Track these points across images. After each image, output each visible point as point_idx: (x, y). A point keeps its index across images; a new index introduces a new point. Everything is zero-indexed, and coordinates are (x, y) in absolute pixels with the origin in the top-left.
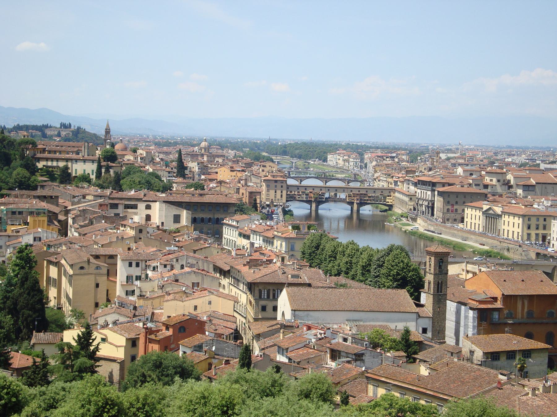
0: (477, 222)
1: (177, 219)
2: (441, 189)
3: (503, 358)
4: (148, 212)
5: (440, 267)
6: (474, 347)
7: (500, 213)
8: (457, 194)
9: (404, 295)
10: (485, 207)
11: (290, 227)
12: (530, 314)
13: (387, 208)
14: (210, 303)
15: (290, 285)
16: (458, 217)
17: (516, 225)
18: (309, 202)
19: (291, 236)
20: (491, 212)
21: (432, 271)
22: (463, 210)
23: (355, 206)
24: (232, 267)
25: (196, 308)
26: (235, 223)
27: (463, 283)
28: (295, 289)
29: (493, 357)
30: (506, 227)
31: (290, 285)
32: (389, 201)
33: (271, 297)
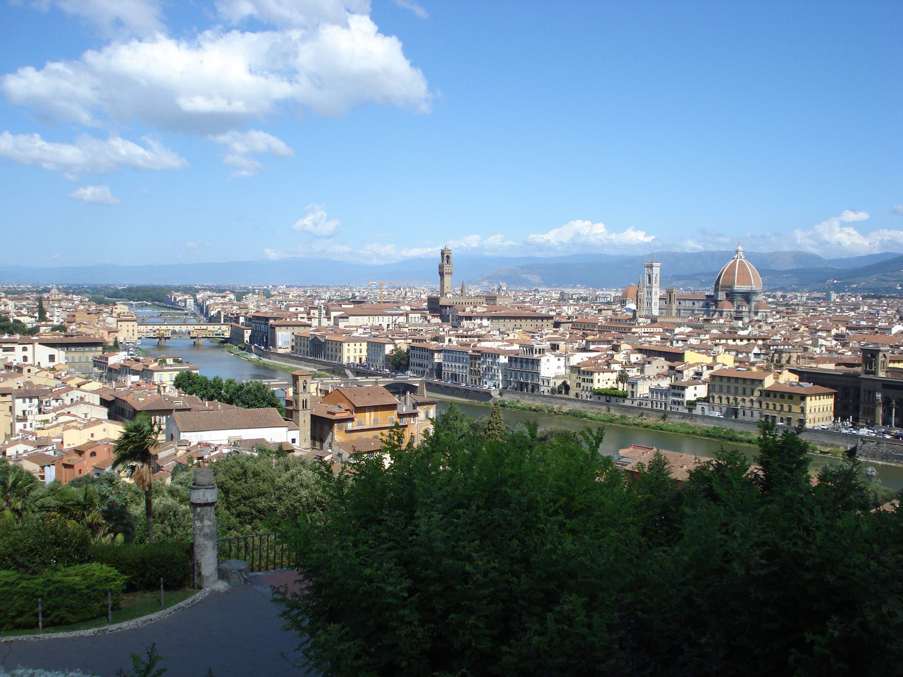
1: (52, 358)
4: (25, 354)
12: (376, 420)
24: (116, 398)
25: (92, 435)
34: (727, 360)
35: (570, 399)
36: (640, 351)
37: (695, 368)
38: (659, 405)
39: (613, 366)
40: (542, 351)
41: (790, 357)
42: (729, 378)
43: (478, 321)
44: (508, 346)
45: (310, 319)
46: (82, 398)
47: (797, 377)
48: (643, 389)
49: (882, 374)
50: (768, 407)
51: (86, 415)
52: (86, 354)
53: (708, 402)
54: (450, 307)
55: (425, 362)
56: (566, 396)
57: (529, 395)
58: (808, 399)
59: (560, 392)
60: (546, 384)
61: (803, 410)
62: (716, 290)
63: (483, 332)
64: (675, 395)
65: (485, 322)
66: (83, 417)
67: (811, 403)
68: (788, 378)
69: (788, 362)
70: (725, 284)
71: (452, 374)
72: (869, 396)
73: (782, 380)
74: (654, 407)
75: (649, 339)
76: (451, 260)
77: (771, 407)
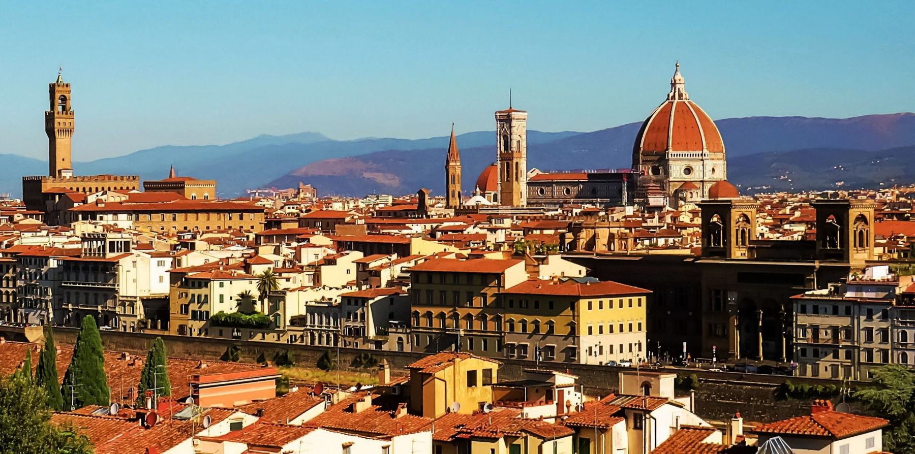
38: (324, 339)
39: (254, 267)
41: (594, 237)
42: (443, 274)
43: (109, 219)
47: (584, 270)
48: (294, 306)
49: (739, 253)
53: (409, 326)
54: (60, 195)
58: (583, 303)
59: (154, 327)
60: (129, 311)
61: (573, 333)
62: (636, 163)
67: (590, 314)
68: (558, 268)
69: (591, 244)
70: (652, 148)
72: (718, 301)
73: (546, 272)
74: (317, 343)
76: (72, 104)
77: (519, 328)
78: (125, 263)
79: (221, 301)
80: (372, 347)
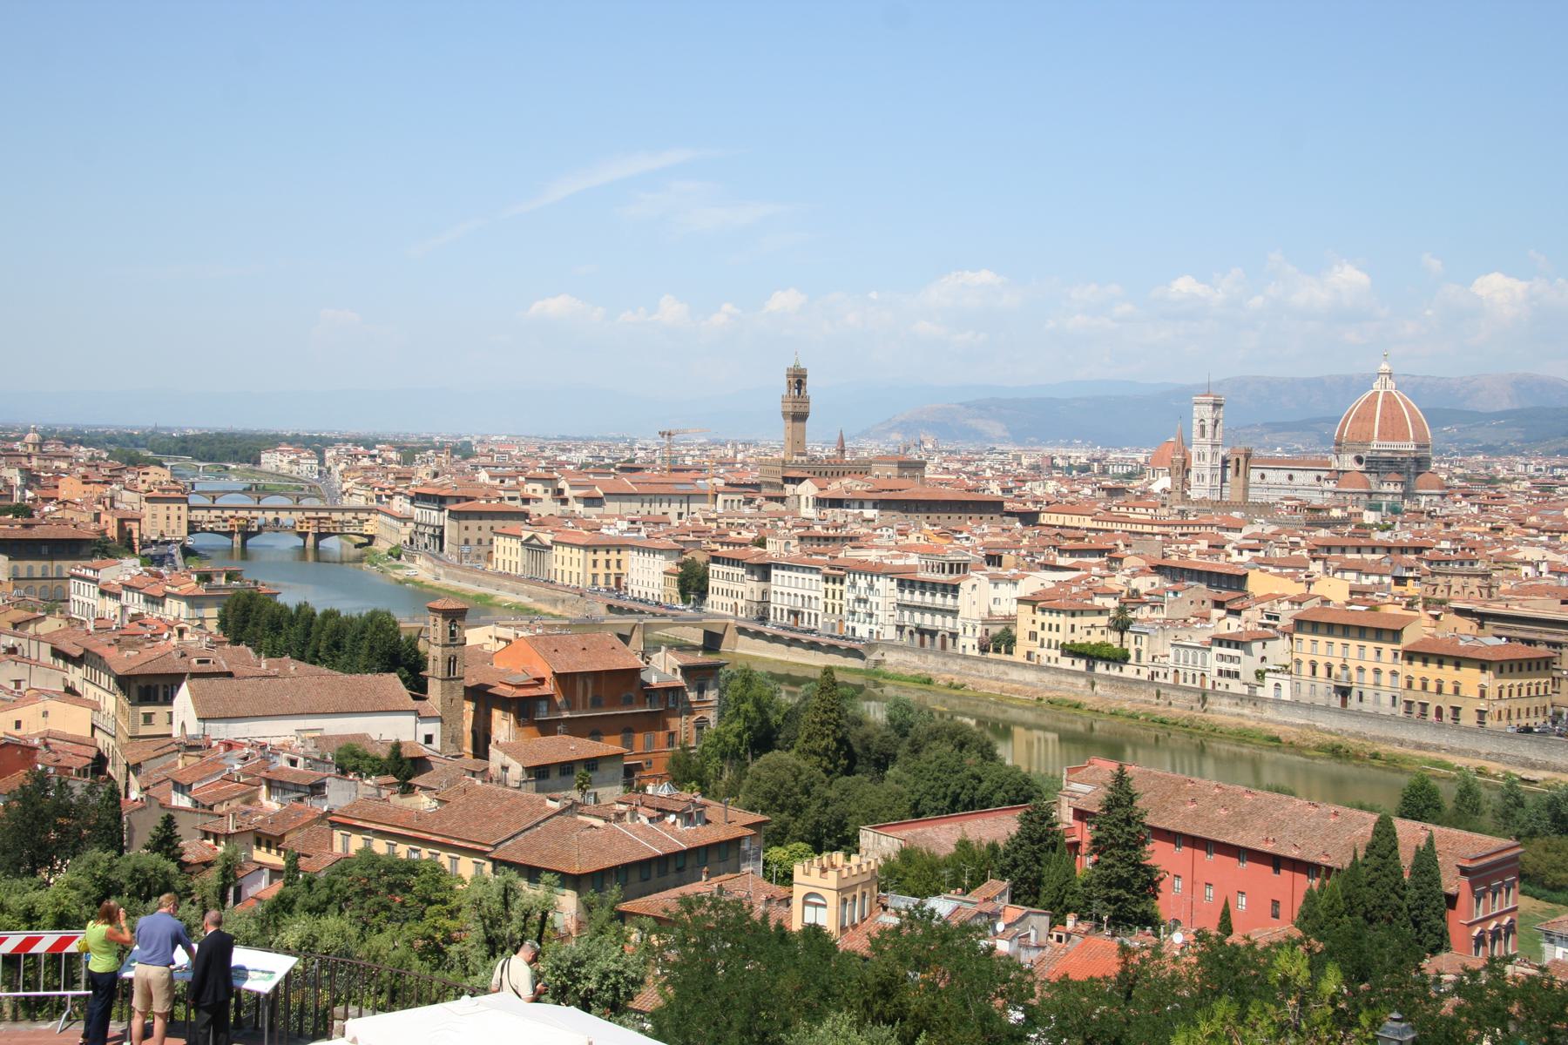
0: (514, 559)
2: (455, 507)
3: (555, 775)
5: (452, 633)
6: (508, 761)
7: (549, 543)
8: (480, 515)
9: (393, 683)
10: (526, 535)
11: (194, 577)
13: (365, 540)
14: (45, 714)
15: (194, 675)
16: (483, 551)
17: (575, 562)
18: (230, 534)
19: (197, 593)
20: (534, 541)
21: (439, 641)
22: (491, 542)
23: (311, 540)
24: (86, 650)
25: (18, 724)
26: (90, 574)
27: (489, 658)
28: (204, 681)
29: (539, 774)
30: (558, 566)
31: (194, 675)
32: (369, 529)
33: (161, 699)
34: (1335, 589)
35: (1015, 664)
36: (1159, 569)
37: (1266, 606)
38: (1190, 679)
40: (960, 568)
44: (900, 557)
45: (526, 501)
46: (13, 650)
50: (1410, 685)
51: (18, 683)
52: (57, 563)
55: (739, 587)
56: (1008, 658)
57: (936, 654)
59: (997, 650)
63: (863, 531)
64: (1222, 658)
65: (870, 513)
66: (13, 685)
71: (790, 612)
74: (1181, 683)
75: (1183, 547)
78: (965, 586)
79: (1073, 630)
80: (1245, 690)
